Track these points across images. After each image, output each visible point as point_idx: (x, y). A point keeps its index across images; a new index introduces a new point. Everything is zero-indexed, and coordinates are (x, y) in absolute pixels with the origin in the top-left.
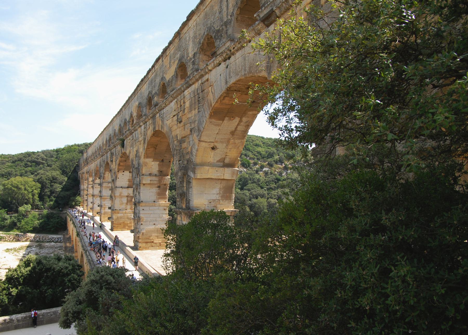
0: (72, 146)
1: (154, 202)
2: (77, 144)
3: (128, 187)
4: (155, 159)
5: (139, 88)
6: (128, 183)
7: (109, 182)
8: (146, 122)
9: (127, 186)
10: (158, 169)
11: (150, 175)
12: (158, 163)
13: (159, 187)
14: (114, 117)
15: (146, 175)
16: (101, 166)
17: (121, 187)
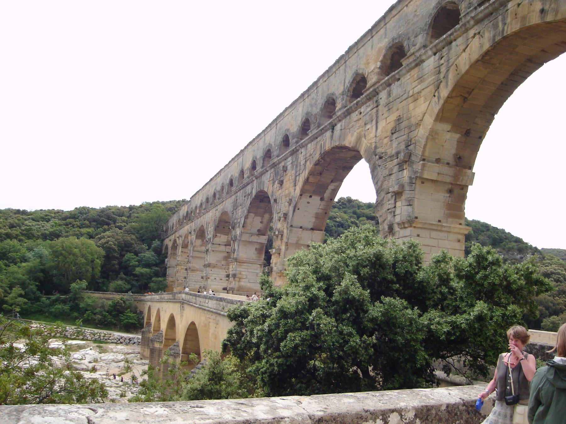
0: (154, 203)
1: (439, 221)
2: (161, 201)
3: (312, 229)
4: (455, 128)
5: (394, 12)
6: (313, 220)
7: (252, 234)
8: (451, 43)
9: (311, 226)
10: (454, 151)
11: (438, 161)
12: (458, 136)
13: (450, 191)
14: (286, 109)
15: (429, 161)
16: (235, 206)
17: (301, 227)
